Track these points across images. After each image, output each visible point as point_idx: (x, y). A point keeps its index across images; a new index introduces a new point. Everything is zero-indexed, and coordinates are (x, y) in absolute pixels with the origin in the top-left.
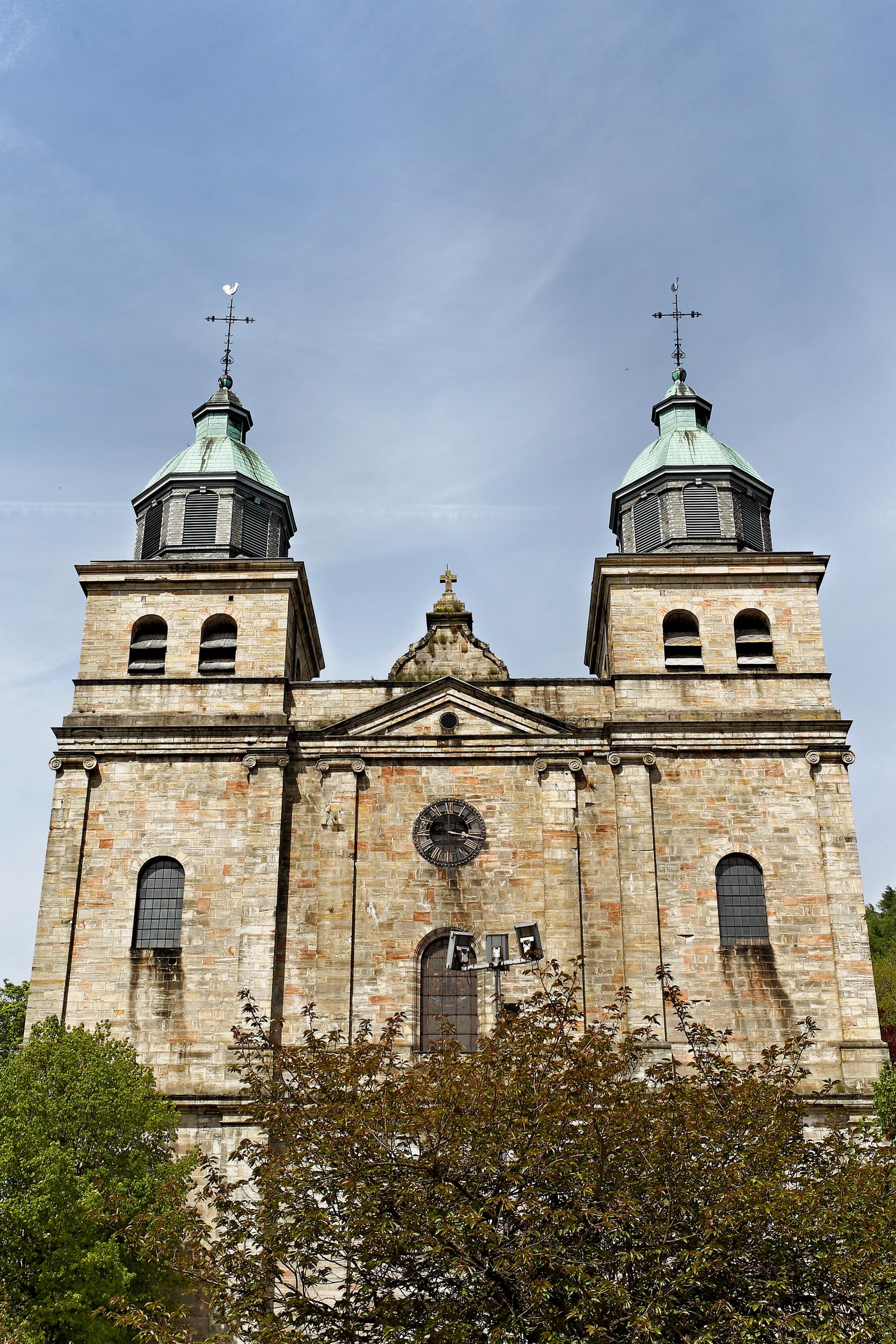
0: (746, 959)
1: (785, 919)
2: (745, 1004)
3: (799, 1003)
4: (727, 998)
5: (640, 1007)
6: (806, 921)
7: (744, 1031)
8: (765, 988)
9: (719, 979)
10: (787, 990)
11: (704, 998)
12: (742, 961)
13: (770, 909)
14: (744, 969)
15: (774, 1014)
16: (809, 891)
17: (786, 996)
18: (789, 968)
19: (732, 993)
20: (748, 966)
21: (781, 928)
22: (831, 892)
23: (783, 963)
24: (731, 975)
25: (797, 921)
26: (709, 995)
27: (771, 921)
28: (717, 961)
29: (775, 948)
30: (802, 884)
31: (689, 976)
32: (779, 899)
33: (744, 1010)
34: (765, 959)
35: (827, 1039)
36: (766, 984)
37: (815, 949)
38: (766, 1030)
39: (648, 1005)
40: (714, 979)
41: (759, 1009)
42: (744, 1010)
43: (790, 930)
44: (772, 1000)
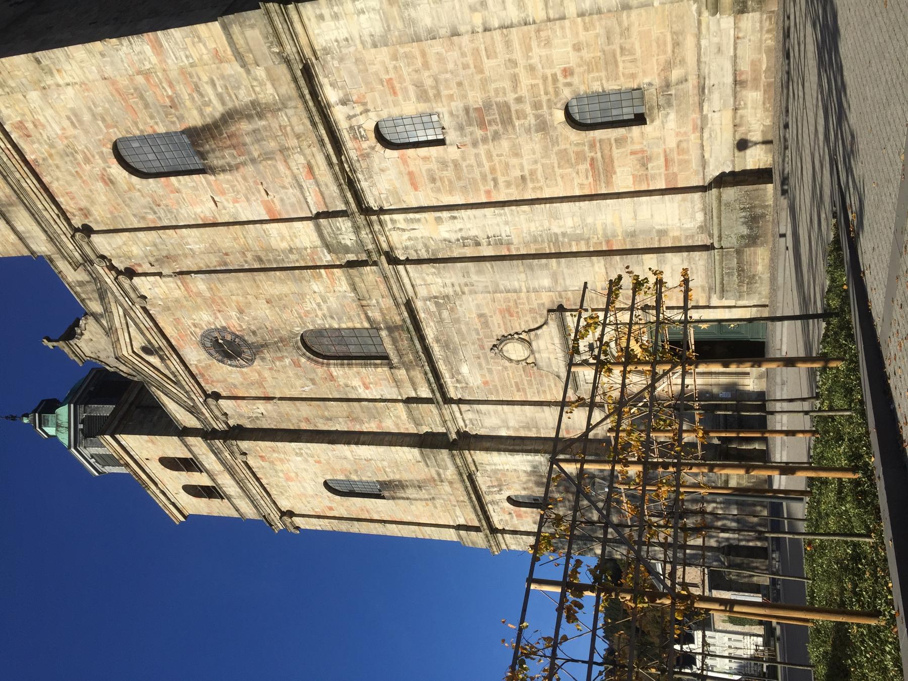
0: (208, 152)
1: (152, 117)
2: (249, 153)
3: (223, 103)
4: (250, 169)
5: (292, 240)
6: (142, 97)
7: (273, 152)
8: (225, 135)
9: (238, 175)
10: (217, 115)
11: (260, 186)
12: (211, 155)
13: (150, 131)
14: (217, 154)
15: (245, 126)
16: (112, 95)
17: (223, 115)
18: (195, 113)
19: (244, 164)
20: (213, 151)
21: (162, 121)
22: (98, 77)
23: (194, 119)
24: (229, 164)
25: (147, 106)
26: (255, 182)
27: (161, 129)
28: (221, 177)
29: (183, 128)
30: (109, 102)
31: (248, 200)
32: (136, 123)
33: (256, 154)
34: (198, 135)
35: (244, 75)
36: (221, 134)
37: (163, 88)
38: (264, 134)
39: (287, 235)
40: (240, 179)
41: (248, 140)
42: (256, 154)
43: (158, 112)
44: (233, 129)
